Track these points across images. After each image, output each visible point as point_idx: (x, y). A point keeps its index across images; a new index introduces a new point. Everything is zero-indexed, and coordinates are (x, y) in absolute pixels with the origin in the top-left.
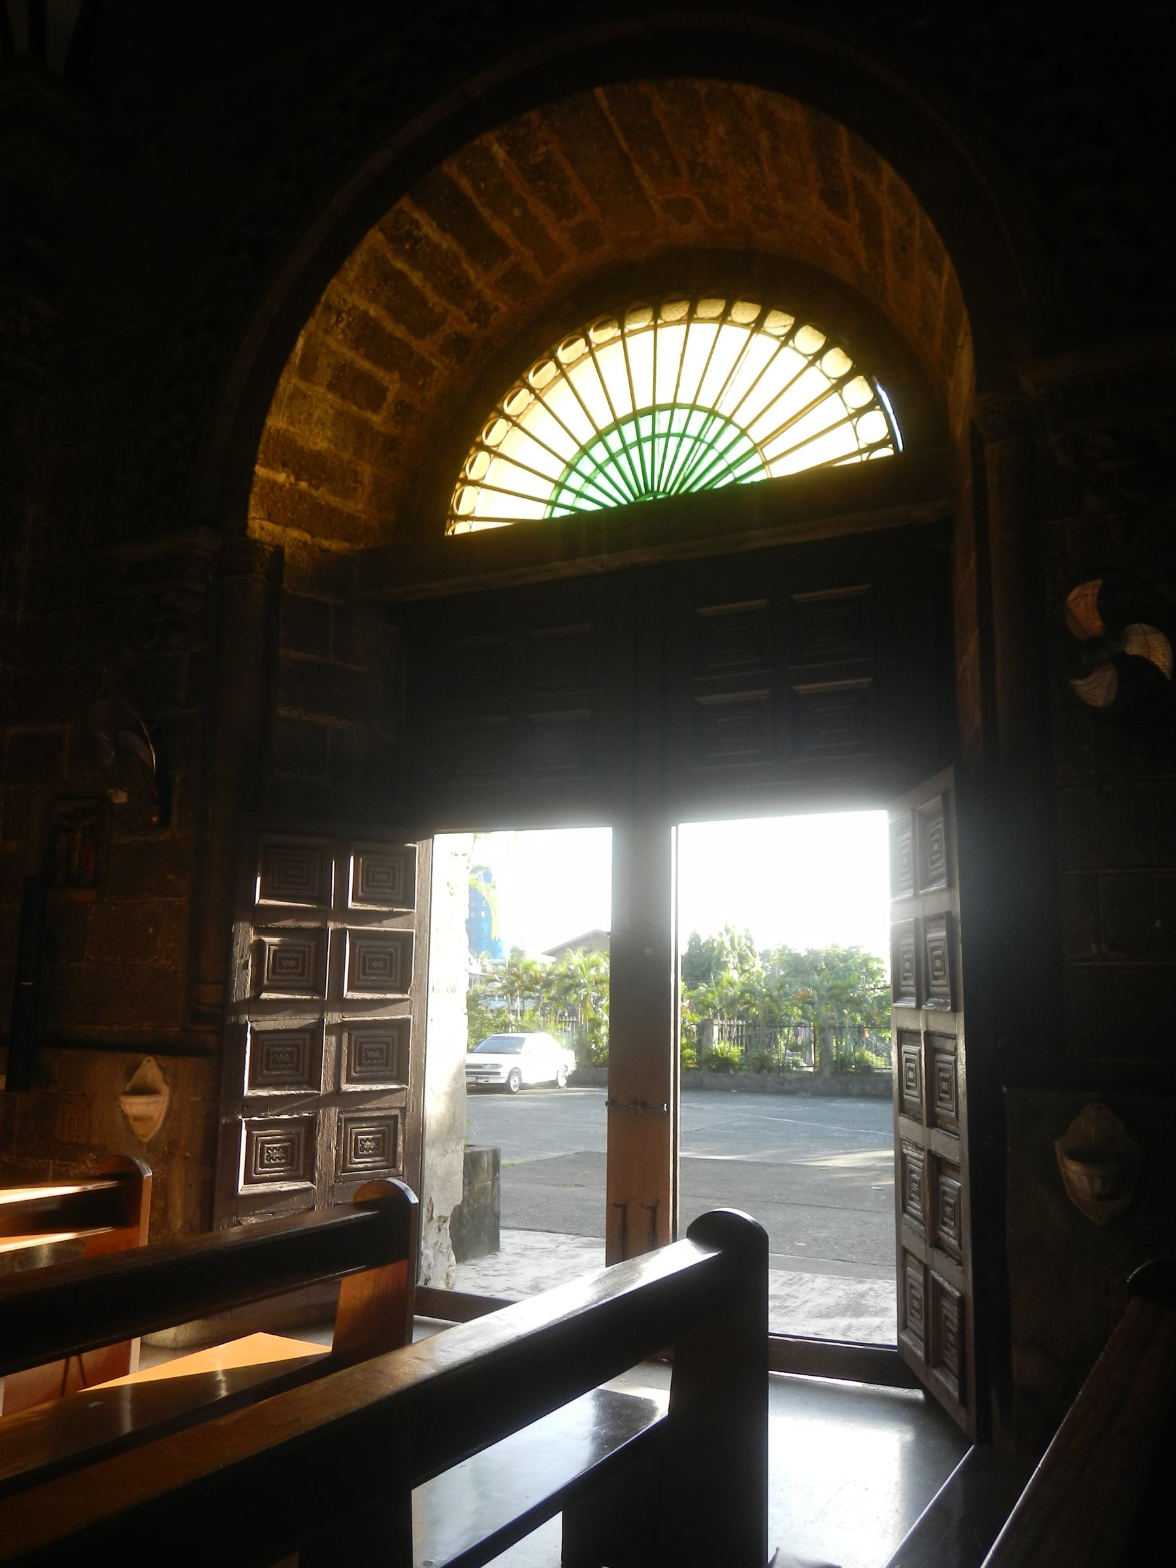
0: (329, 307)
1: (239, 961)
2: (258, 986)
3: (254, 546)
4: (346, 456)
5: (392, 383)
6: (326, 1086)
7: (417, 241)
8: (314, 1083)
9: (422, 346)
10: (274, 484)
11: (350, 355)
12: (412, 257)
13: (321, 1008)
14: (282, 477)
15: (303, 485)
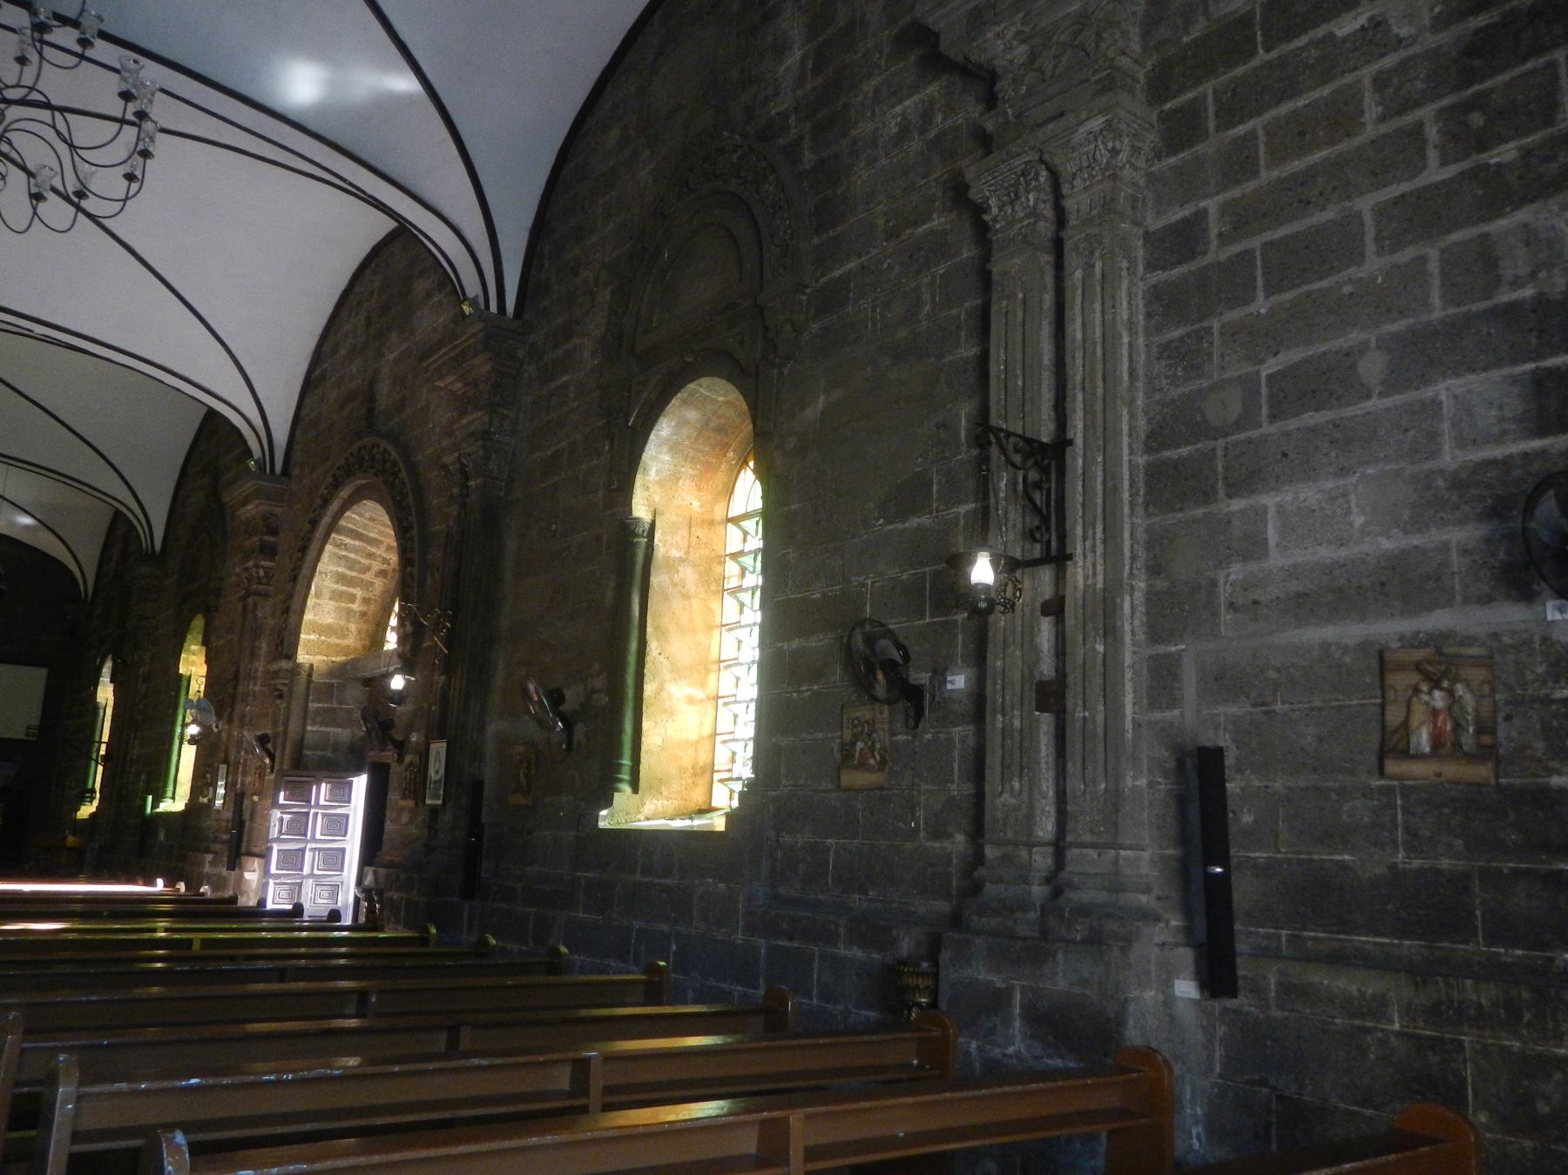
0: (321, 573)
1: (272, 824)
2: (280, 832)
3: (299, 666)
4: (342, 623)
5: (358, 592)
6: (306, 870)
7: (346, 545)
8: (301, 870)
9: (368, 577)
10: (309, 641)
11: (335, 586)
12: (346, 549)
13: (307, 842)
14: (312, 637)
15: (323, 638)
